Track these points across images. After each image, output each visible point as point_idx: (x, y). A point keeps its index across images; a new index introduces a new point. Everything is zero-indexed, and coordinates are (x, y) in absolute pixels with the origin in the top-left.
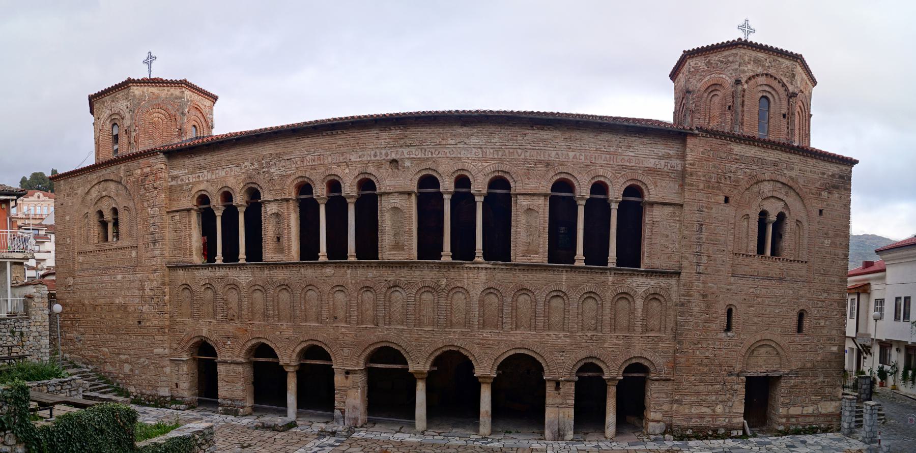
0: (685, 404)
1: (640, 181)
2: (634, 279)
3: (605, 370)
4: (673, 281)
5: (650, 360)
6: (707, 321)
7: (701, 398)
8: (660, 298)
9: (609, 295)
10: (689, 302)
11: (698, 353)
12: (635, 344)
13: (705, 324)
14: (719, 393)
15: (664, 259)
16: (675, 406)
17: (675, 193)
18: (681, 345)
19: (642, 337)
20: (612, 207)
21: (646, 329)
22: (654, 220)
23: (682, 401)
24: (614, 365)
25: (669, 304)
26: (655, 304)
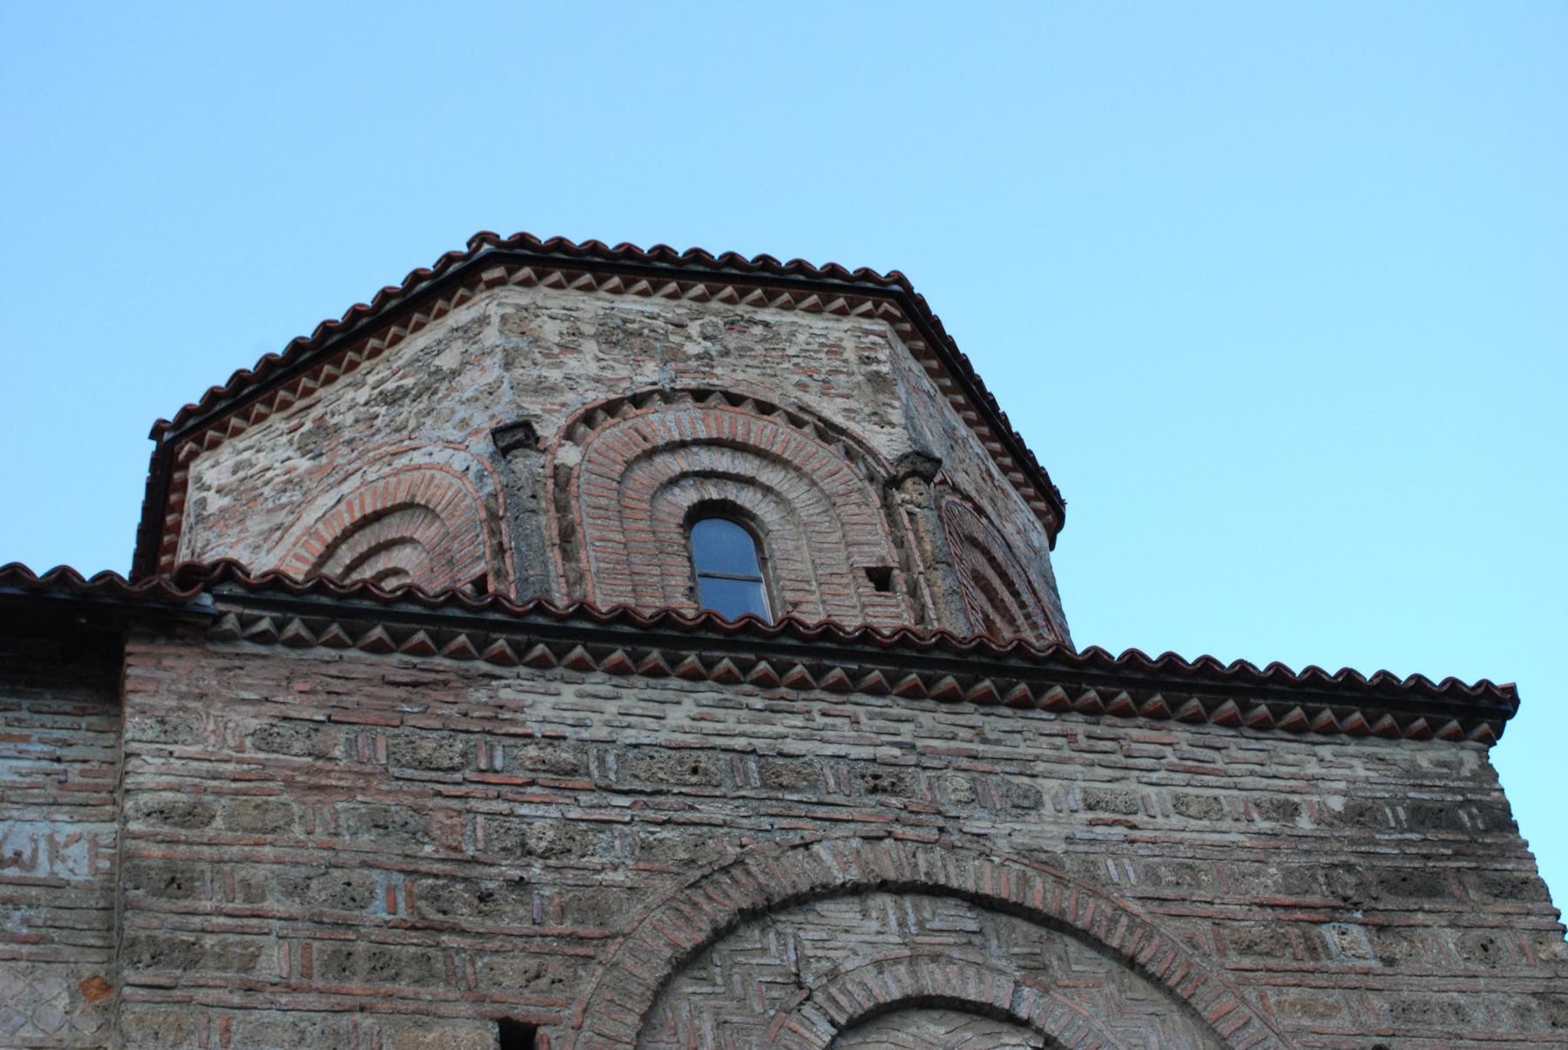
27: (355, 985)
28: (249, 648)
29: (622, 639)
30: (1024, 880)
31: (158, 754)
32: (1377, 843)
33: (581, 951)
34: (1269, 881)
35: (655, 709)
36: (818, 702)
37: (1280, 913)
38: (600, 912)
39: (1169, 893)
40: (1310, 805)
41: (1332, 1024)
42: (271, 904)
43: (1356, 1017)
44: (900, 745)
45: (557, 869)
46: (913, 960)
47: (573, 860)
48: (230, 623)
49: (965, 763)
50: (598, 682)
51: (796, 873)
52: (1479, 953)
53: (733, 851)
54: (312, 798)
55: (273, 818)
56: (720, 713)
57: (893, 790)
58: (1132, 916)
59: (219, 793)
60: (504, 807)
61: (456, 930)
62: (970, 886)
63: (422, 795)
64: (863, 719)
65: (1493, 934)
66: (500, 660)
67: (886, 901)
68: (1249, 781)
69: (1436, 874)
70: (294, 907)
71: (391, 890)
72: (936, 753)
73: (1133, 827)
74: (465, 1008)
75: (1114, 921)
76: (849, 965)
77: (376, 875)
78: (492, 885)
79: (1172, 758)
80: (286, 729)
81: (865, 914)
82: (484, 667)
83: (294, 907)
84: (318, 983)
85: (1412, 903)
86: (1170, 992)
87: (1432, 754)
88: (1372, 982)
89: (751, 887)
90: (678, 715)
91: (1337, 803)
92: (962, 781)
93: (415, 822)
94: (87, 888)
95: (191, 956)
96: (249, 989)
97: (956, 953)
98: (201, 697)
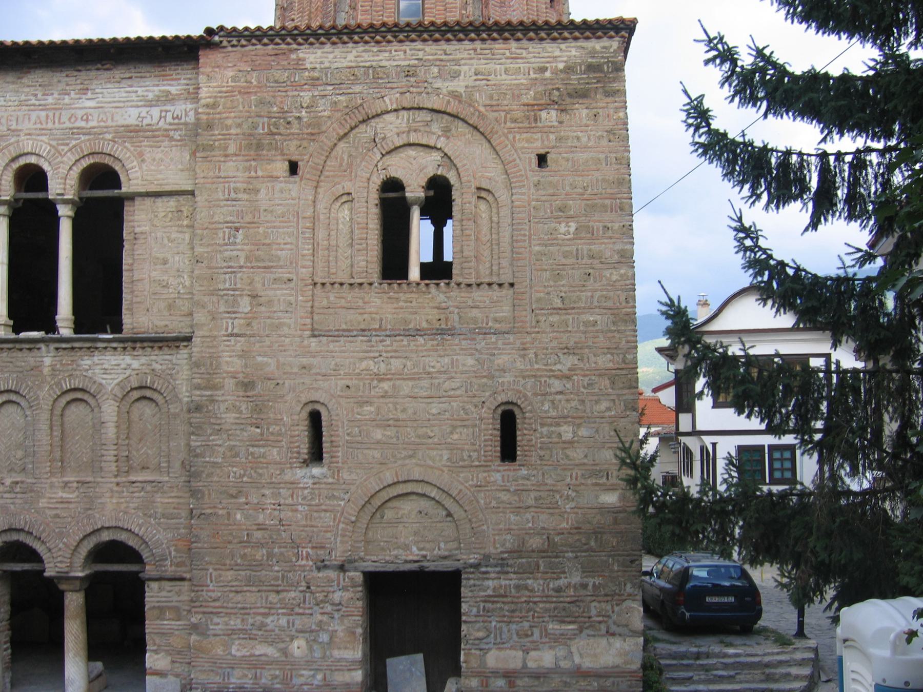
0: (215, 635)
1: (110, 155)
2: (96, 359)
3: (45, 556)
4: (181, 357)
5: (137, 535)
6: (254, 442)
7: (251, 621)
8: (155, 396)
9: (46, 395)
10: (213, 401)
11: (239, 516)
12: (103, 500)
13: (251, 449)
14: (297, 610)
15: (159, 311)
16: (194, 638)
17: (182, 171)
18: (198, 499)
19: (118, 484)
20: (60, 213)
21: (126, 465)
22: (137, 230)
23: (209, 629)
24: (61, 545)
25: (174, 408)
26: (147, 409)
27: (252, 153)
28: (230, 49)
29: (334, 34)
30: (449, 102)
31: (207, 87)
32: (571, 80)
33: (313, 138)
34: (529, 97)
35: (344, 55)
36: (395, 46)
37: (530, 108)
38: (319, 125)
39: (494, 103)
40: (552, 67)
41: (535, 145)
42: (233, 131)
43: (543, 141)
44: (417, 59)
45: (309, 112)
46: (409, 132)
47: (313, 109)
48: (225, 43)
49: (438, 63)
50: (328, 47)
51: (379, 107)
52: (593, 117)
53: (359, 102)
54: (245, 96)
55: (236, 104)
56: (363, 54)
57: (413, 75)
58: (479, 112)
59: (221, 97)
60: (296, 93)
61: (280, 134)
62: (430, 106)
63: (275, 92)
64: (408, 51)
65: (600, 111)
66: (300, 44)
67: (405, 113)
68: (533, 60)
69: (588, 90)
70: (238, 131)
71: (263, 124)
72: (429, 60)
73: (488, 80)
74: (279, 157)
75: (473, 114)
76: (389, 135)
77: (261, 120)
78: (290, 119)
79: (508, 54)
80: (240, 74)
81: (398, 118)
82: (295, 46)
83: (238, 131)
84: (243, 153)
85: (576, 101)
86: (486, 137)
87: (602, 44)
88: (552, 130)
89: (364, 112)
90: (351, 57)
91: (561, 66)
92: (436, 70)
93: (272, 100)
94: (194, 124)
95: (211, 148)
96: (226, 156)
97: (422, 129)
98: (218, 67)
